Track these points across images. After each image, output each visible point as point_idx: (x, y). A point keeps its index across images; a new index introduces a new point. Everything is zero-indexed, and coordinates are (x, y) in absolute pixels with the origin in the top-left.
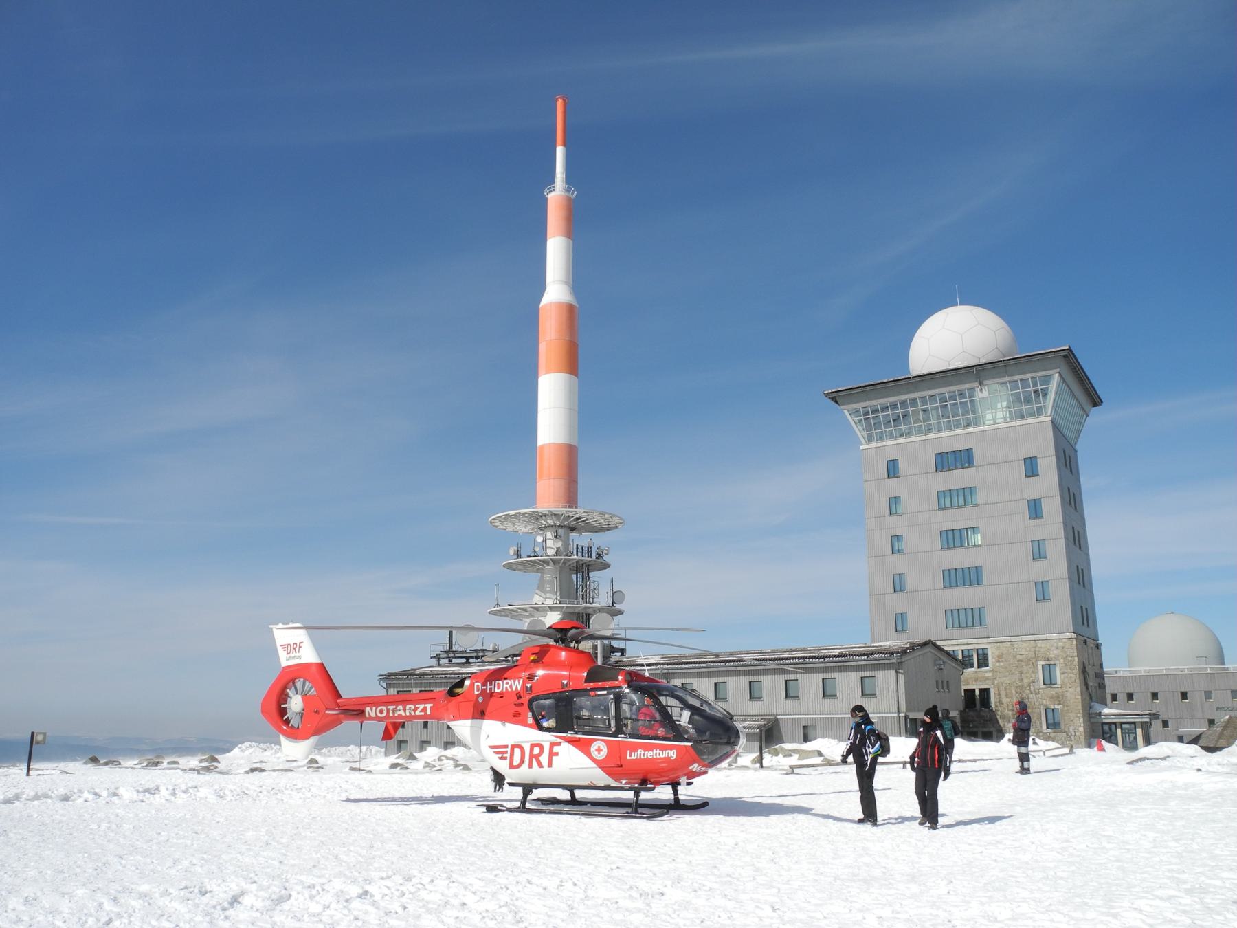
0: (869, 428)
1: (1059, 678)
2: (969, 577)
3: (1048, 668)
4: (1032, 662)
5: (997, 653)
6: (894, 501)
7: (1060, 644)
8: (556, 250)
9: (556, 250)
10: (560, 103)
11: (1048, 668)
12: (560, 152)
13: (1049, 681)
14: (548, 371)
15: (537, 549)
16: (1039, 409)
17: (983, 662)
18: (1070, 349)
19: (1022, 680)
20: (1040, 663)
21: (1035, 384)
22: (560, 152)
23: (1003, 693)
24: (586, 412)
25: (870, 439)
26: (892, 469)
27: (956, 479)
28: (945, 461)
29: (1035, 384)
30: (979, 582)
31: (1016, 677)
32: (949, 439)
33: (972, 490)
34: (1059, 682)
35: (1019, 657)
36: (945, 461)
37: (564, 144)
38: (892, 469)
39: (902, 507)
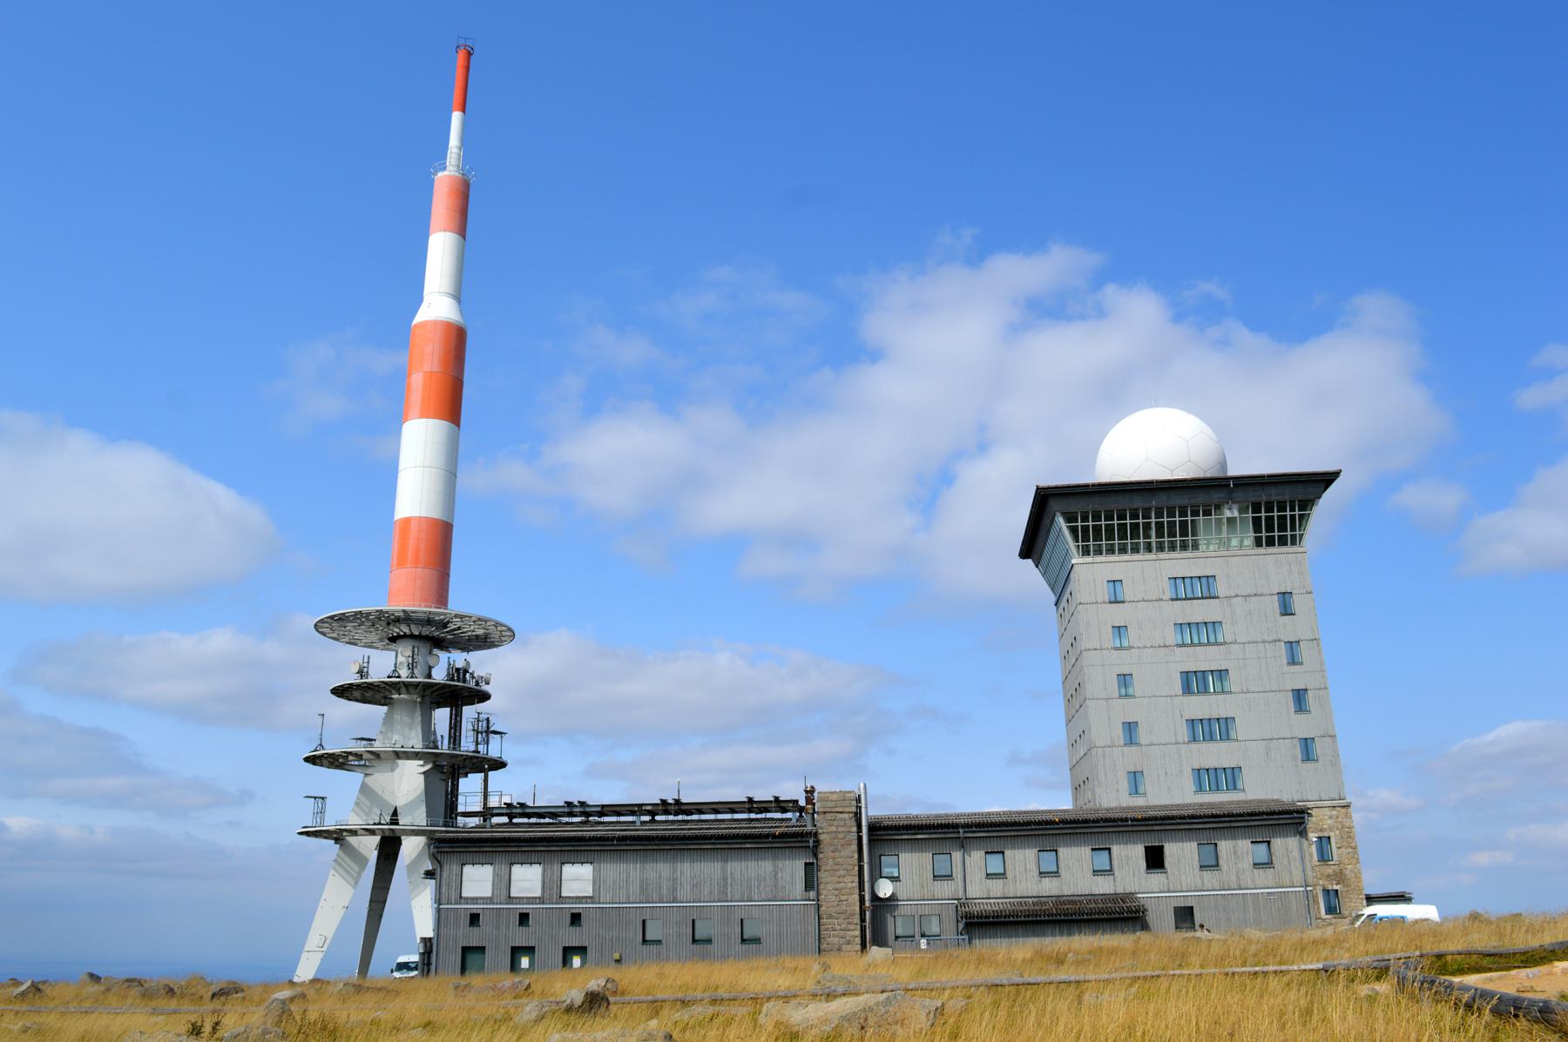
0: (1086, 538)
6: (1119, 630)
14: (424, 415)
21: (1293, 509)
25: (1086, 552)
27: (1200, 611)
29: (1293, 509)
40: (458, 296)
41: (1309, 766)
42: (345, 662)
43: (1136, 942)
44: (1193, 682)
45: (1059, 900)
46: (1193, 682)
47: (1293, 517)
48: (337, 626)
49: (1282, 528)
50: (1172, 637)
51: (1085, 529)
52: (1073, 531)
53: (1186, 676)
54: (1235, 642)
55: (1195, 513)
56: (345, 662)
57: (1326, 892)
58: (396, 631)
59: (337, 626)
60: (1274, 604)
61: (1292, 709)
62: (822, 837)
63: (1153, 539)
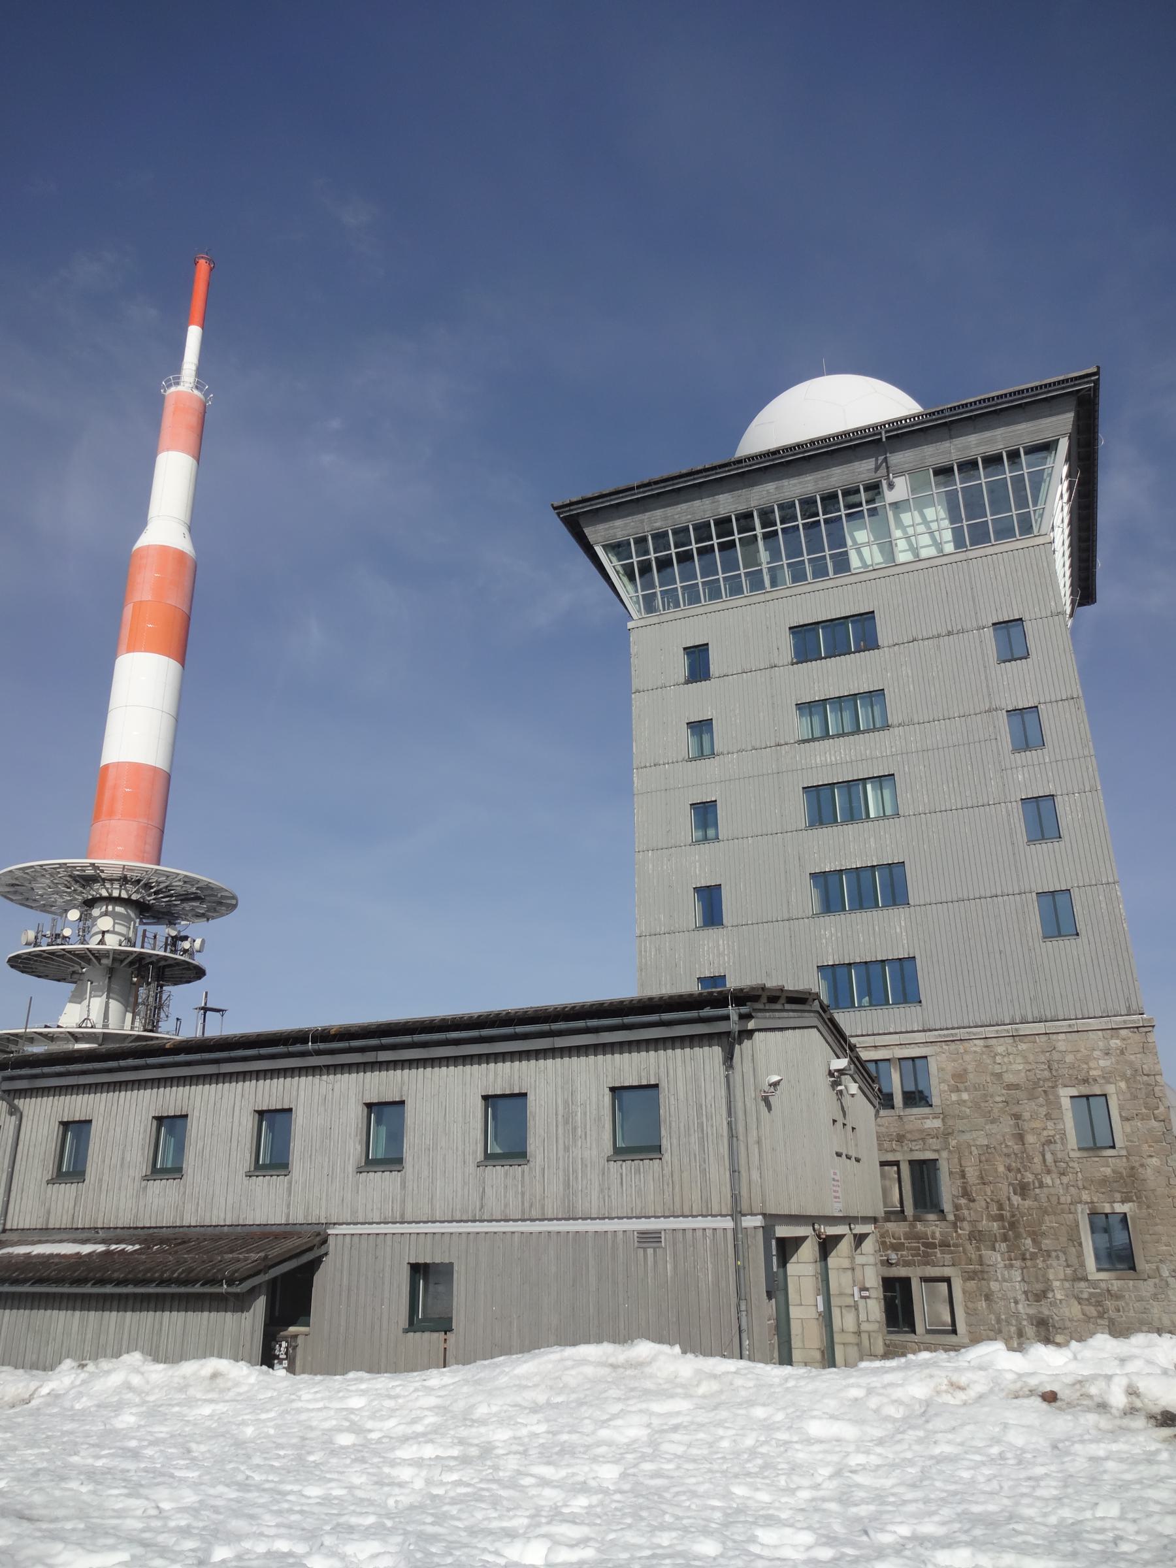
2: (878, 887)
4: (1041, 1088)
5: (950, 1067)
6: (701, 728)
7: (1115, 1043)
8: (173, 475)
9: (173, 475)
10: (203, 265)
12: (194, 334)
19: (1020, 1138)
22: (194, 334)
23: (972, 1174)
24: (189, 716)
26: (698, 662)
31: (1006, 1126)
33: (875, 696)
35: (1009, 1078)
39: (721, 737)
40: (196, 525)
42: (24, 932)
44: (829, 803)
45: (177, 1239)
46: (829, 803)
47: (1018, 481)
49: (1000, 503)
50: (799, 726)
52: (629, 573)
57: (1101, 1223)
58: (90, 894)
59: (20, 890)
61: (1021, 834)
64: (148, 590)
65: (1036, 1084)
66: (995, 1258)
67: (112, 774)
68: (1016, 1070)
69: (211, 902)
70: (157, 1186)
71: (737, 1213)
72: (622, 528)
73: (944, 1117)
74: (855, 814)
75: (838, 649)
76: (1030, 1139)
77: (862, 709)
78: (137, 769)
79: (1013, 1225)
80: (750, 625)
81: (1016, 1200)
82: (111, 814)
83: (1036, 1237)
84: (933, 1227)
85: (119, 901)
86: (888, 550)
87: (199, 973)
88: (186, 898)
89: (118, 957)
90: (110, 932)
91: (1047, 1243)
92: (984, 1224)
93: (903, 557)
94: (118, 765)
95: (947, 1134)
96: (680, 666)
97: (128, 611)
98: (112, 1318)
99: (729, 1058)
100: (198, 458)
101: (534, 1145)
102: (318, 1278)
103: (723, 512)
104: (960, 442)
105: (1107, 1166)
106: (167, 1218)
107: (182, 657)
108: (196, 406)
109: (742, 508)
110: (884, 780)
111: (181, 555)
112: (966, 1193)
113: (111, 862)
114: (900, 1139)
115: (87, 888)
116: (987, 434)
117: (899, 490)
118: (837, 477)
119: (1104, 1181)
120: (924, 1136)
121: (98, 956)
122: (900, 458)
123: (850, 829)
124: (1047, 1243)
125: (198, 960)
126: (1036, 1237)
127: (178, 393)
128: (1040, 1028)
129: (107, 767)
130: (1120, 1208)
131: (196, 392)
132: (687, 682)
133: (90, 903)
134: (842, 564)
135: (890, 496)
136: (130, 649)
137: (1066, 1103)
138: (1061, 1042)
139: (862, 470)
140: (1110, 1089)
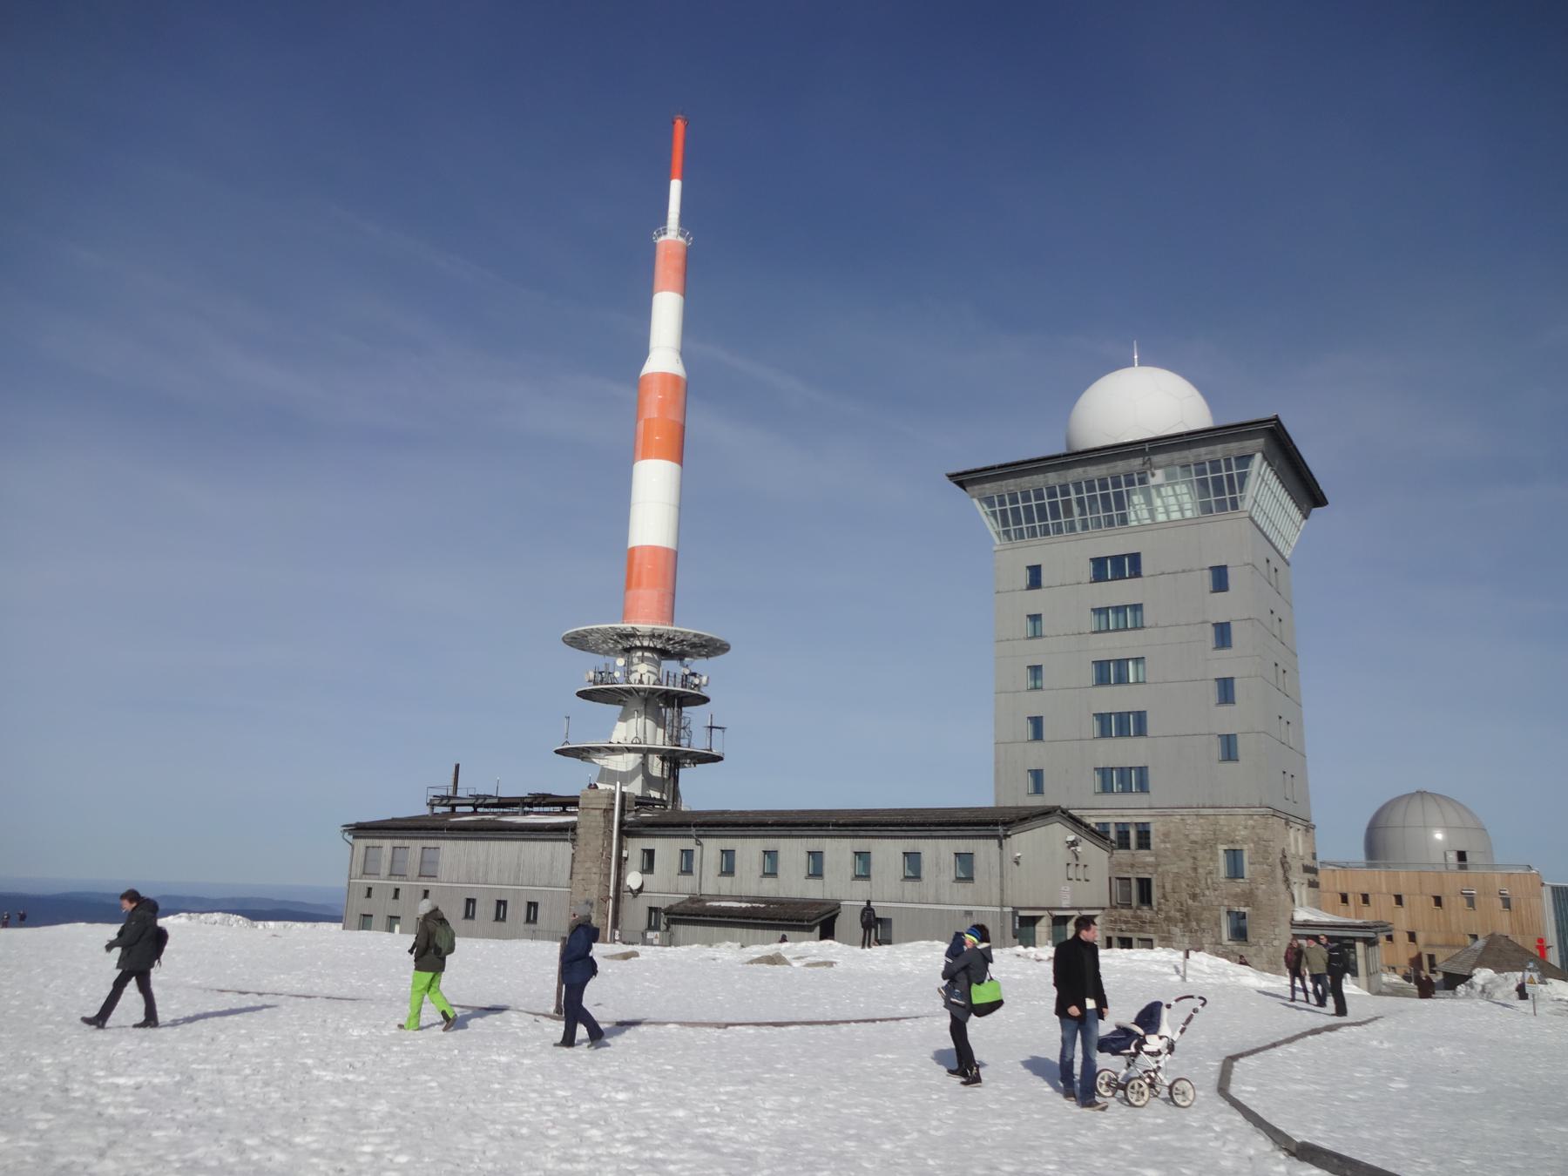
0: (1005, 523)
1: (1247, 869)
2: (1129, 724)
3: (1234, 856)
4: (1209, 844)
6: (1035, 618)
8: (667, 309)
9: (667, 309)
10: (680, 124)
11: (1234, 856)
12: (675, 186)
13: (1235, 872)
15: (617, 674)
16: (1235, 506)
17: (1144, 840)
18: (1276, 419)
19: (1195, 869)
20: (1221, 848)
21: (1229, 468)
22: (675, 186)
23: (1168, 887)
24: (690, 506)
26: (1035, 577)
27: (1118, 592)
28: (1103, 569)
29: (1229, 468)
30: (1141, 731)
31: (1189, 863)
32: (1112, 544)
33: (1137, 608)
34: (1246, 874)
35: (1193, 837)
36: (1103, 569)
37: (683, 179)
38: (1035, 577)
41: (1229, 765)
42: (585, 669)
43: (889, 953)
46: (1109, 672)
47: (1230, 478)
48: (578, 641)
50: (1091, 622)
51: (1004, 513)
52: (994, 513)
53: (1101, 666)
54: (1156, 626)
55: (1130, 483)
56: (585, 669)
58: (627, 644)
59: (578, 641)
60: (1207, 578)
62: (579, 831)
63: (1077, 517)
64: (654, 406)
65: (1206, 842)
66: (1176, 931)
67: (637, 554)
68: (1197, 833)
69: (711, 647)
70: (767, 880)
71: (1002, 906)
72: (990, 488)
73: (1157, 856)
74: (1122, 679)
75: (1119, 575)
76: (1200, 870)
77: (1129, 616)
78: (654, 550)
79: (1187, 915)
80: (1068, 554)
81: (1190, 902)
82: (639, 585)
83: (1198, 921)
84: (1146, 913)
85: (648, 649)
86: (1152, 512)
87: (705, 700)
88: (693, 645)
89: (652, 692)
90: (644, 673)
91: (1203, 925)
92: (1172, 913)
93: (1161, 517)
94: (642, 547)
95: (1157, 865)
96: (1024, 578)
97: (641, 424)
98: (759, 932)
99: (1001, 845)
100: (684, 295)
101: (923, 874)
102: (837, 920)
103: (1051, 483)
104: (1195, 451)
105: (1239, 886)
106: (772, 894)
107: (681, 463)
108: (681, 251)
109: (1062, 482)
110: (1138, 660)
111: (676, 378)
112: (1164, 897)
113: (644, 627)
114: (1132, 866)
115: (626, 644)
116: (1211, 448)
117: (1159, 477)
118: (1121, 467)
119: (1236, 895)
120: (1146, 865)
121: (638, 691)
122: (1158, 459)
123: (1118, 688)
124: (1203, 925)
125: (705, 692)
126: (1198, 921)
127: (667, 242)
128: (1211, 811)
129: (633, 549)
130: (1243, 909)
131: (681, 239)
132: (1029, 588)
133: (628, 650)
134: (1124, 520)
135: (1153, 481)
136: (643, 458)
137: (1221, 853)
138: (1222, 820)
139: (1136, 463)
140: (1245, 847)
